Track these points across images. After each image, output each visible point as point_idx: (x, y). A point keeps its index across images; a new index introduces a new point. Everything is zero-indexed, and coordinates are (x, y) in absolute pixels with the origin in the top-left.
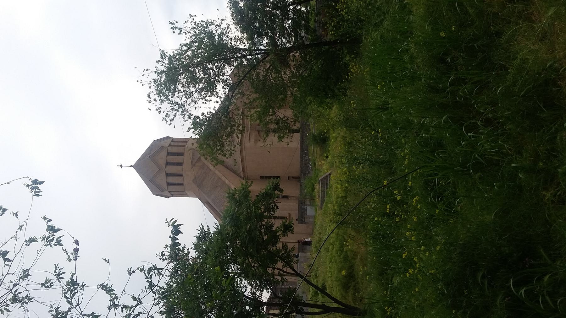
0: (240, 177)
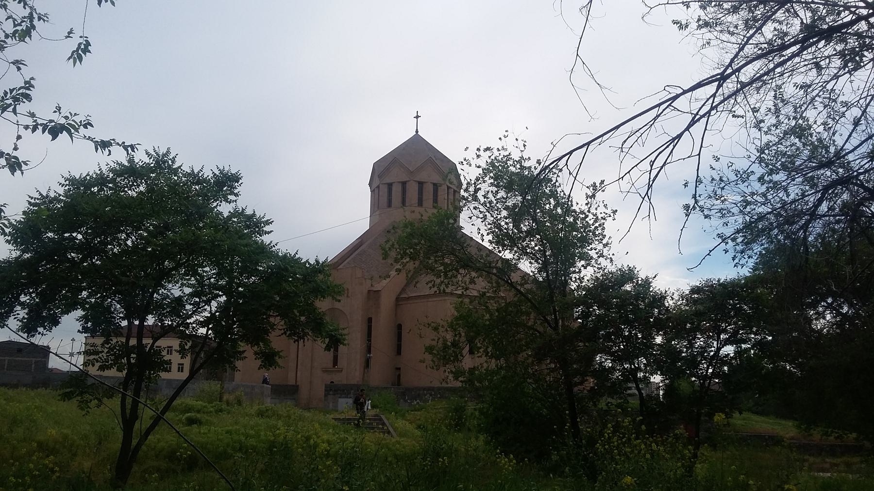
0: (401, 293)
